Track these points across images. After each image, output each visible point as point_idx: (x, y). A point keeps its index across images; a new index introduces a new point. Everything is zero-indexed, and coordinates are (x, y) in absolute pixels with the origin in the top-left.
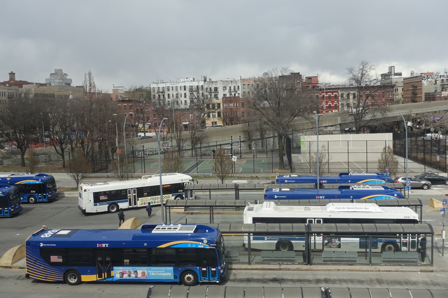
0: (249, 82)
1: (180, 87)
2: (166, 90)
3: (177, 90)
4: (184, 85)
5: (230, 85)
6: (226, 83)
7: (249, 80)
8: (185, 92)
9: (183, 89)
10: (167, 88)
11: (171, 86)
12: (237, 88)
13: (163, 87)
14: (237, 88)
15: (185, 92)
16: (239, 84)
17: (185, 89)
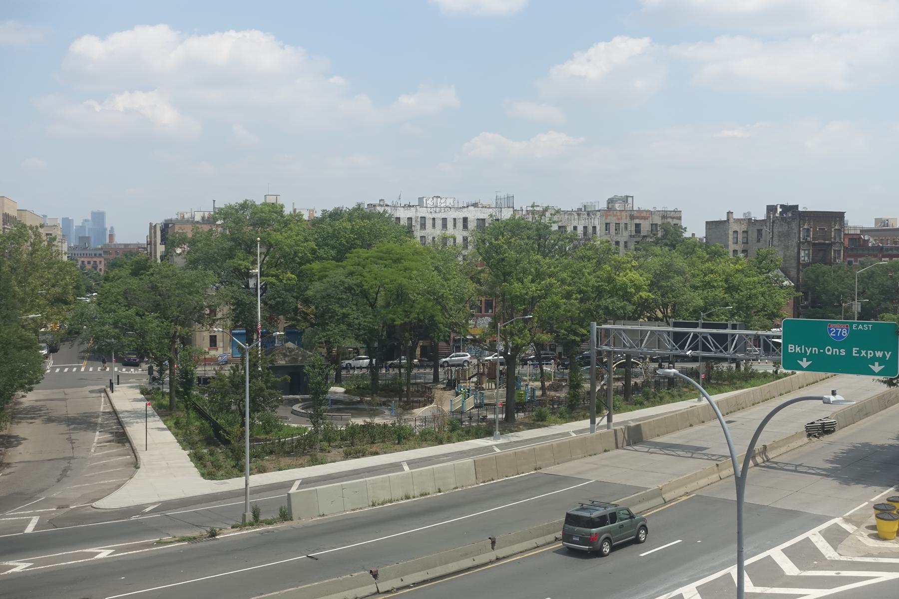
0: (619, 219)
1: (452, 221)
2: (417, 226)
3: (445, 226)
4: (464, 216)
5: (575, 223)
6: (566, 216)
7: (619, 214)
8: (465, 234)
9: (460, 224)
10: (419, 220)
11: (429, 216)
12: (590, 230)
13: (408, 218)
14: (590, 230)
15: (465, 234)
16: (597, 223)
17: (465, 226)
